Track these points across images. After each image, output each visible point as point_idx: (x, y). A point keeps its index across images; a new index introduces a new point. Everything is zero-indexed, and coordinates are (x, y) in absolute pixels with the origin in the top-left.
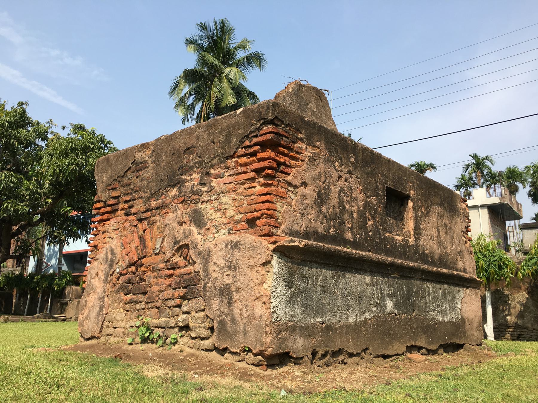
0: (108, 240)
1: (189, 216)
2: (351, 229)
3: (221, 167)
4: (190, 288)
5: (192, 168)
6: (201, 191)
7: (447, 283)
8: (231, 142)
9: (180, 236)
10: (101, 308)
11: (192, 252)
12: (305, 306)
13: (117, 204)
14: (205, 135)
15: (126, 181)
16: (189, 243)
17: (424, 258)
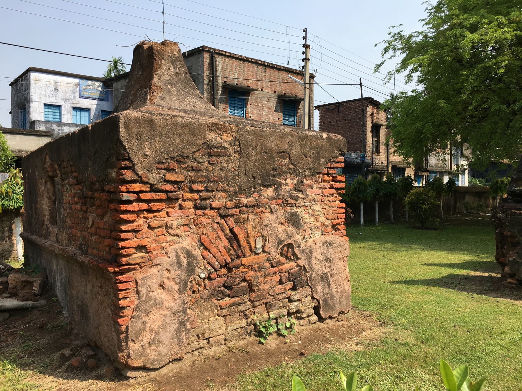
0: (169, 238)
1: (286, 218)
3: (312, 179)
4: (297, 281)
5: (285, 172)
6: (299, 197)
8: (320, 161)
9: (283, 237)
10: (182, 324)
11: (296, 250)
13: (175, 192)
14: (297, 145)
15: (191, 164)
16: (293, 243)
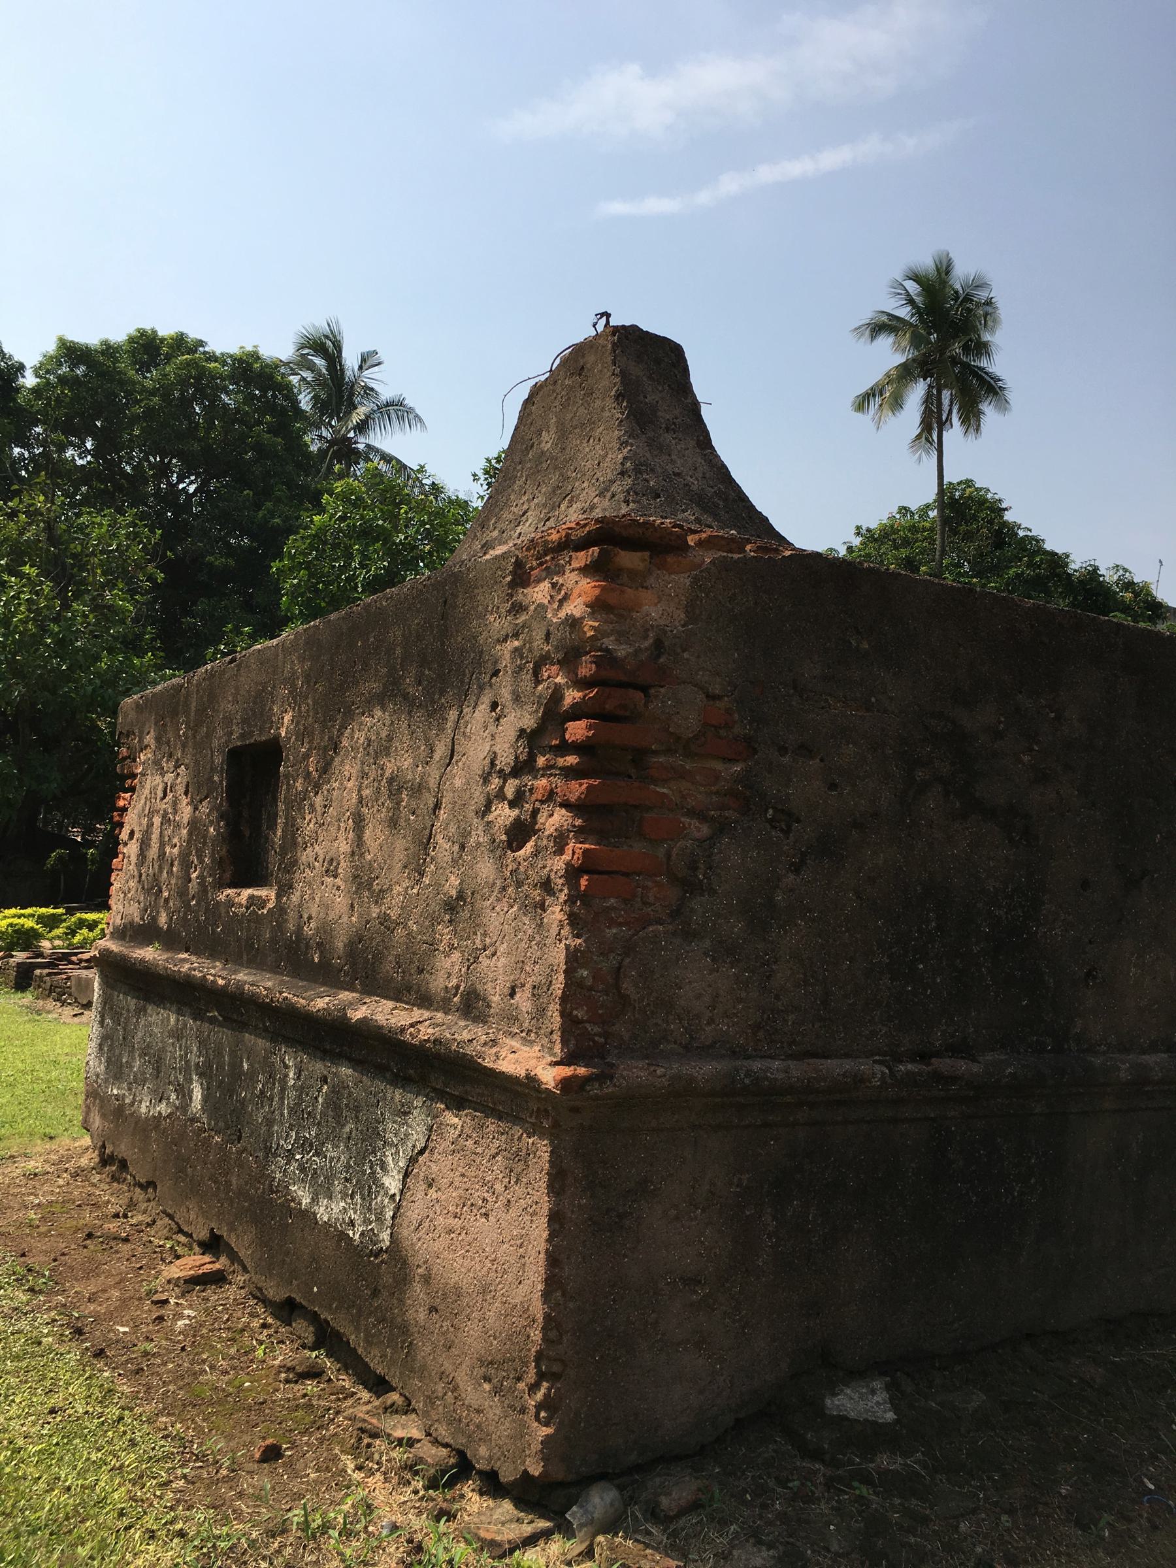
2: (167, 900)
7: (357, 1063)
12: (109, 1060)
17: (296, 956)
